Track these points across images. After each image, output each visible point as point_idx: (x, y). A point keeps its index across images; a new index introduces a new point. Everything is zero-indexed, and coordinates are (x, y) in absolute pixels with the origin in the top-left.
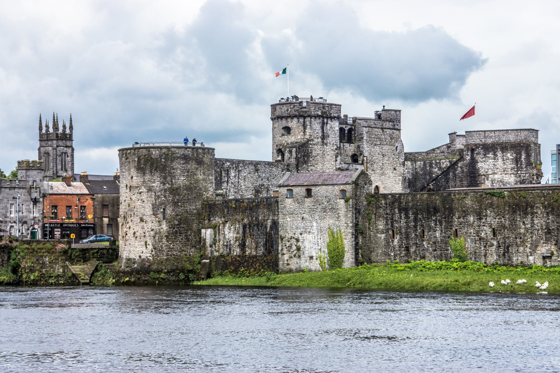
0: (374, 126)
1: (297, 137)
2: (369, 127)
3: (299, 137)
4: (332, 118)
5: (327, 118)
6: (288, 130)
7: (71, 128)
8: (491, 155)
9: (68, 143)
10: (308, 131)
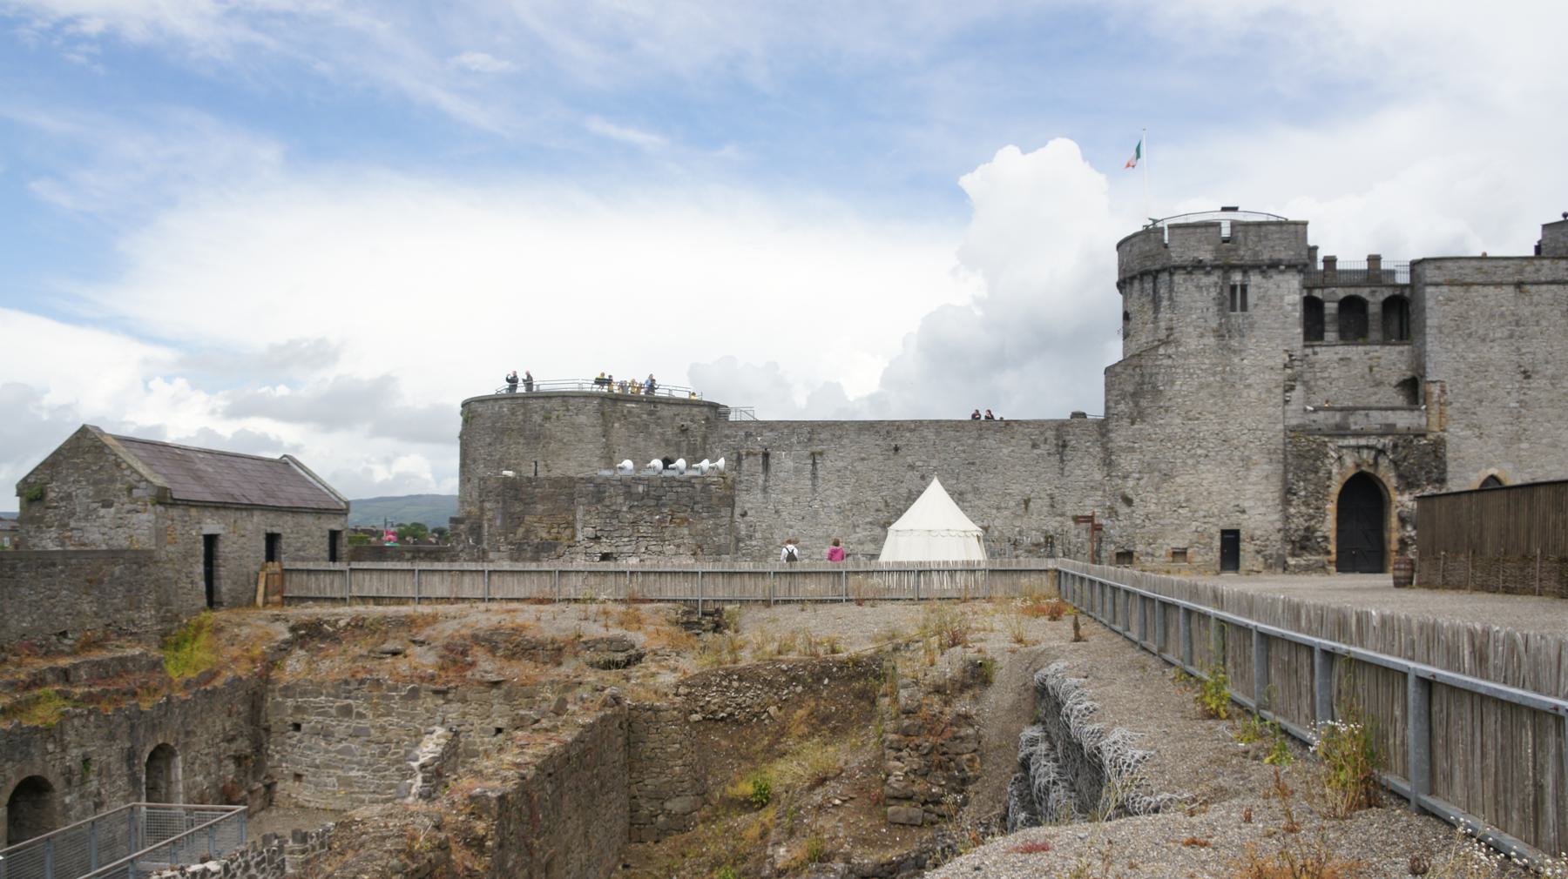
0: (1480, 278)
1: (1143, 339)
2: (1451, 283)
3: (1144, 340)
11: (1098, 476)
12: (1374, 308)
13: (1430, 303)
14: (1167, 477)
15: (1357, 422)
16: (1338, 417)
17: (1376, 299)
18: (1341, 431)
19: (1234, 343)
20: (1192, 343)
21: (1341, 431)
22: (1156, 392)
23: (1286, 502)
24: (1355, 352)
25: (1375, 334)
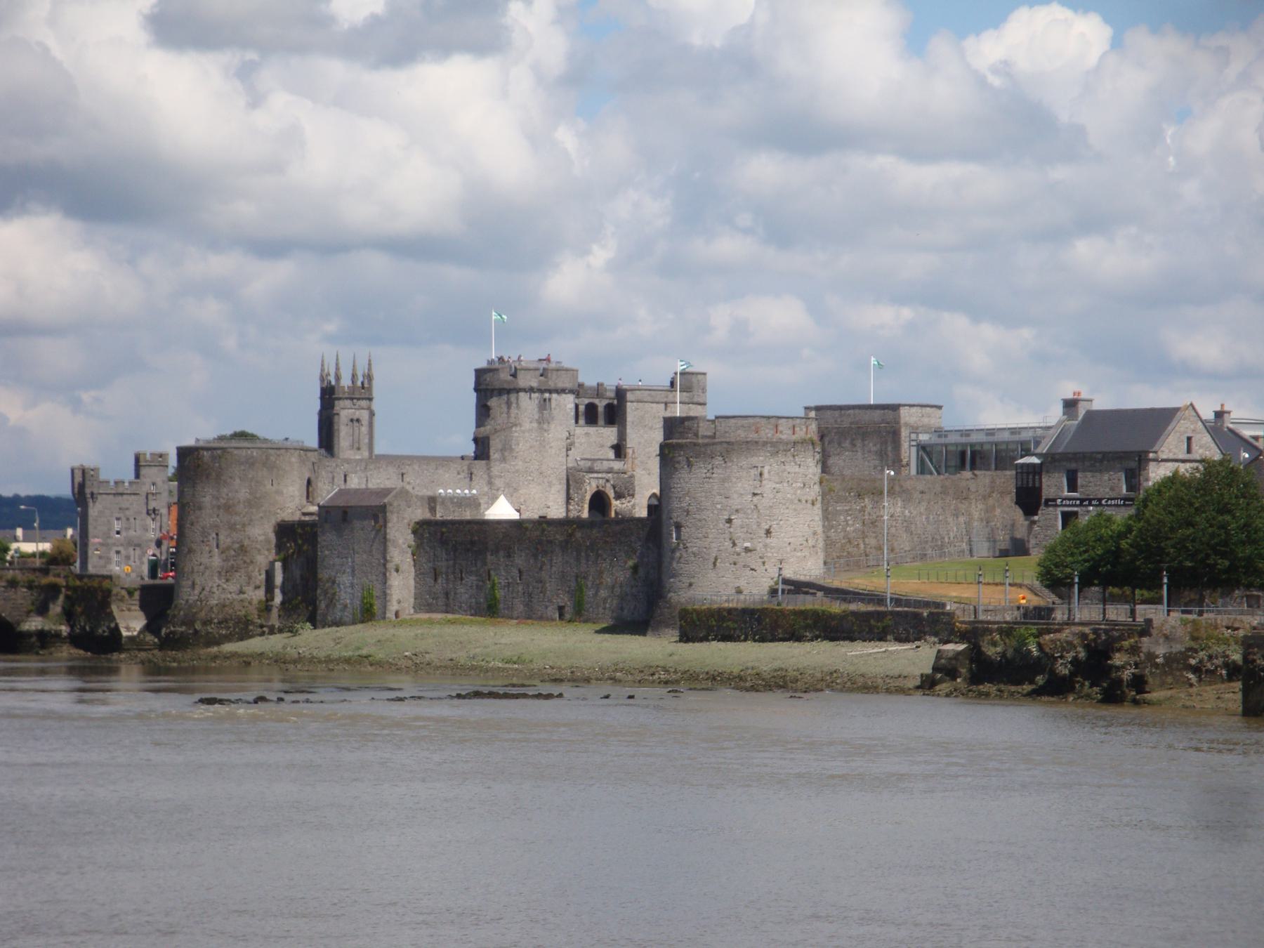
0: (650, 399)
4: (562, 391)
5: (550, 392)
7: (369, 377)
8: (847, 444)
9: (364, 403)
10: (514, 411)
11: (486, 489)
12: (601, 409)
13: (628, 410)
14: (516, 490)
15: (597, 466)
16: (589, 464)
17: (601, 404)
18: (591, 470)
19: (545, 426)
20: (527, 426)
22: (511, 450)
23: (568, 503)
24: (592, 430)
25: (601, 421)
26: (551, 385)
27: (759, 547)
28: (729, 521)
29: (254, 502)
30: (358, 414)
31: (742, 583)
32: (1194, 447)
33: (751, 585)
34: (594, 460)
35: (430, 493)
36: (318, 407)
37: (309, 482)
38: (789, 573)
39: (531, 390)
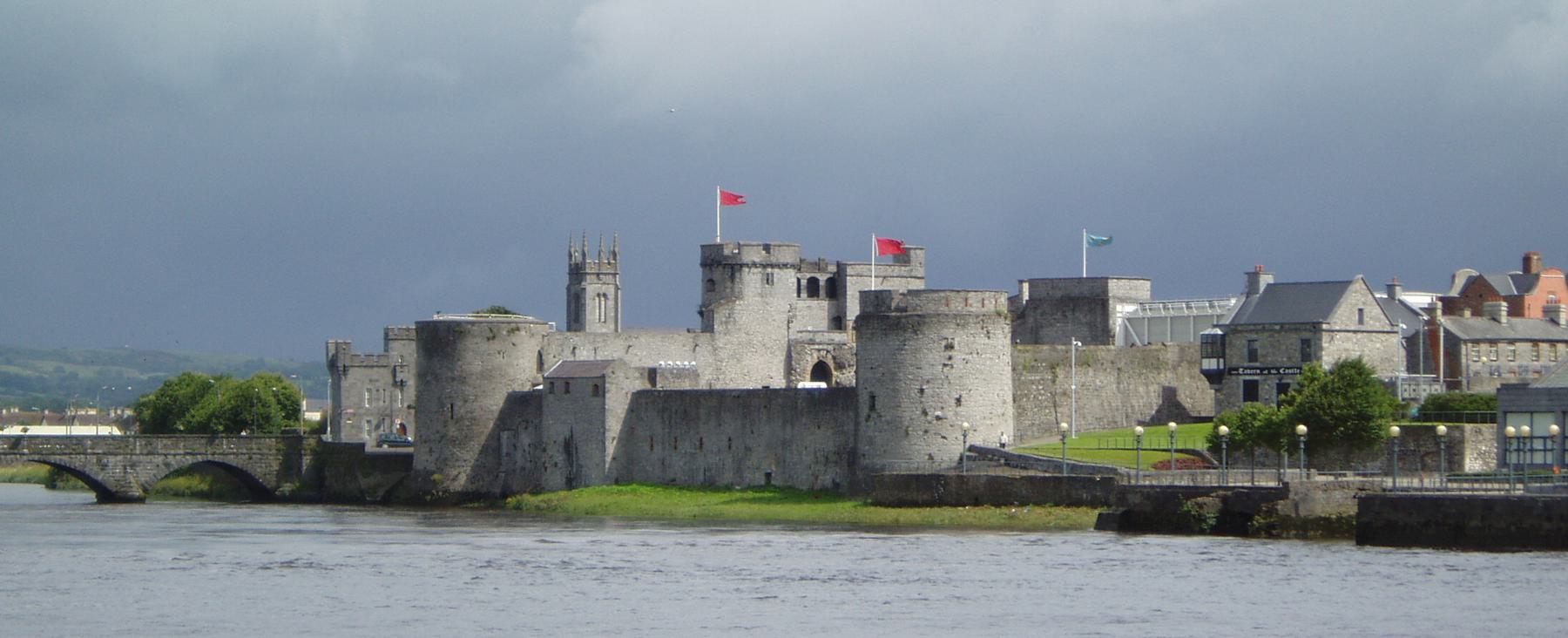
6: (711, 281)
12: (822, 283)
16: (811, 336)
18: (812, 342)
21: (812, 342)
24: (814, 303)
26: (773, 260)
27: (950, 414)
28: (922, 391)
29: (487, 375)
30: (604, 289)
31: (934, 450)
32: (1366, 319)
33: (941, 451)
34: (815, 332)
35: (651, 364)
36: (567, 283)
37: (540, 355)
38: (977, 440)
39: (755, 265)
